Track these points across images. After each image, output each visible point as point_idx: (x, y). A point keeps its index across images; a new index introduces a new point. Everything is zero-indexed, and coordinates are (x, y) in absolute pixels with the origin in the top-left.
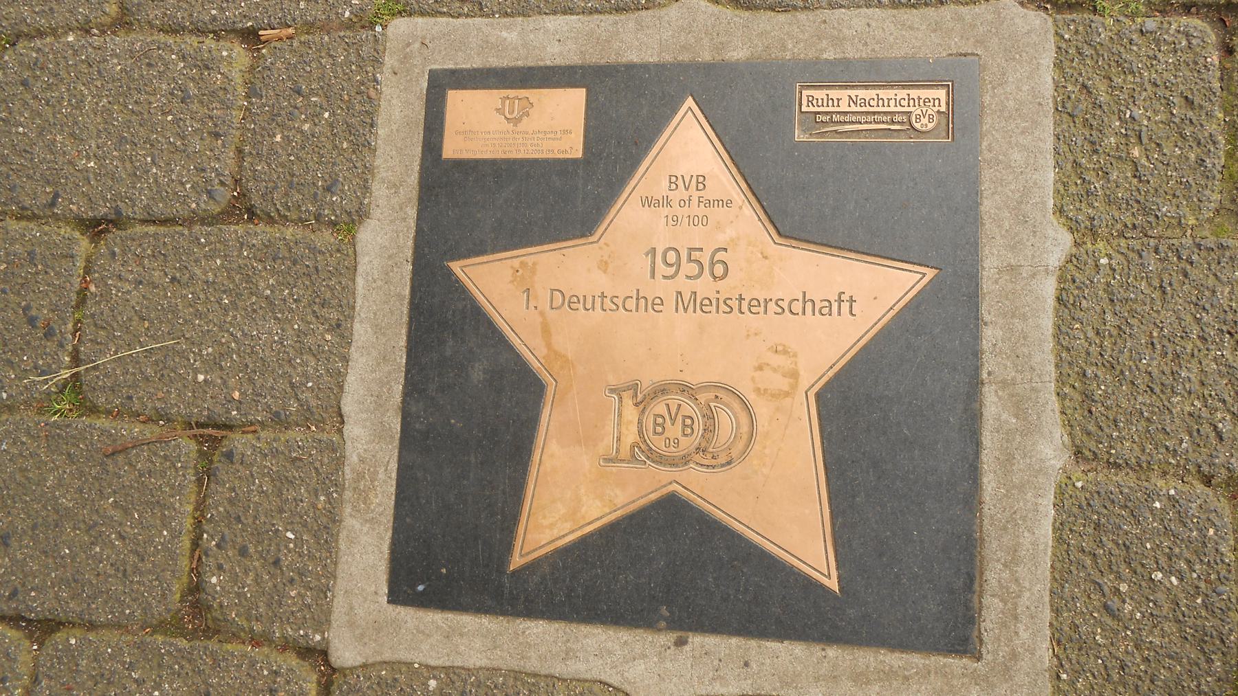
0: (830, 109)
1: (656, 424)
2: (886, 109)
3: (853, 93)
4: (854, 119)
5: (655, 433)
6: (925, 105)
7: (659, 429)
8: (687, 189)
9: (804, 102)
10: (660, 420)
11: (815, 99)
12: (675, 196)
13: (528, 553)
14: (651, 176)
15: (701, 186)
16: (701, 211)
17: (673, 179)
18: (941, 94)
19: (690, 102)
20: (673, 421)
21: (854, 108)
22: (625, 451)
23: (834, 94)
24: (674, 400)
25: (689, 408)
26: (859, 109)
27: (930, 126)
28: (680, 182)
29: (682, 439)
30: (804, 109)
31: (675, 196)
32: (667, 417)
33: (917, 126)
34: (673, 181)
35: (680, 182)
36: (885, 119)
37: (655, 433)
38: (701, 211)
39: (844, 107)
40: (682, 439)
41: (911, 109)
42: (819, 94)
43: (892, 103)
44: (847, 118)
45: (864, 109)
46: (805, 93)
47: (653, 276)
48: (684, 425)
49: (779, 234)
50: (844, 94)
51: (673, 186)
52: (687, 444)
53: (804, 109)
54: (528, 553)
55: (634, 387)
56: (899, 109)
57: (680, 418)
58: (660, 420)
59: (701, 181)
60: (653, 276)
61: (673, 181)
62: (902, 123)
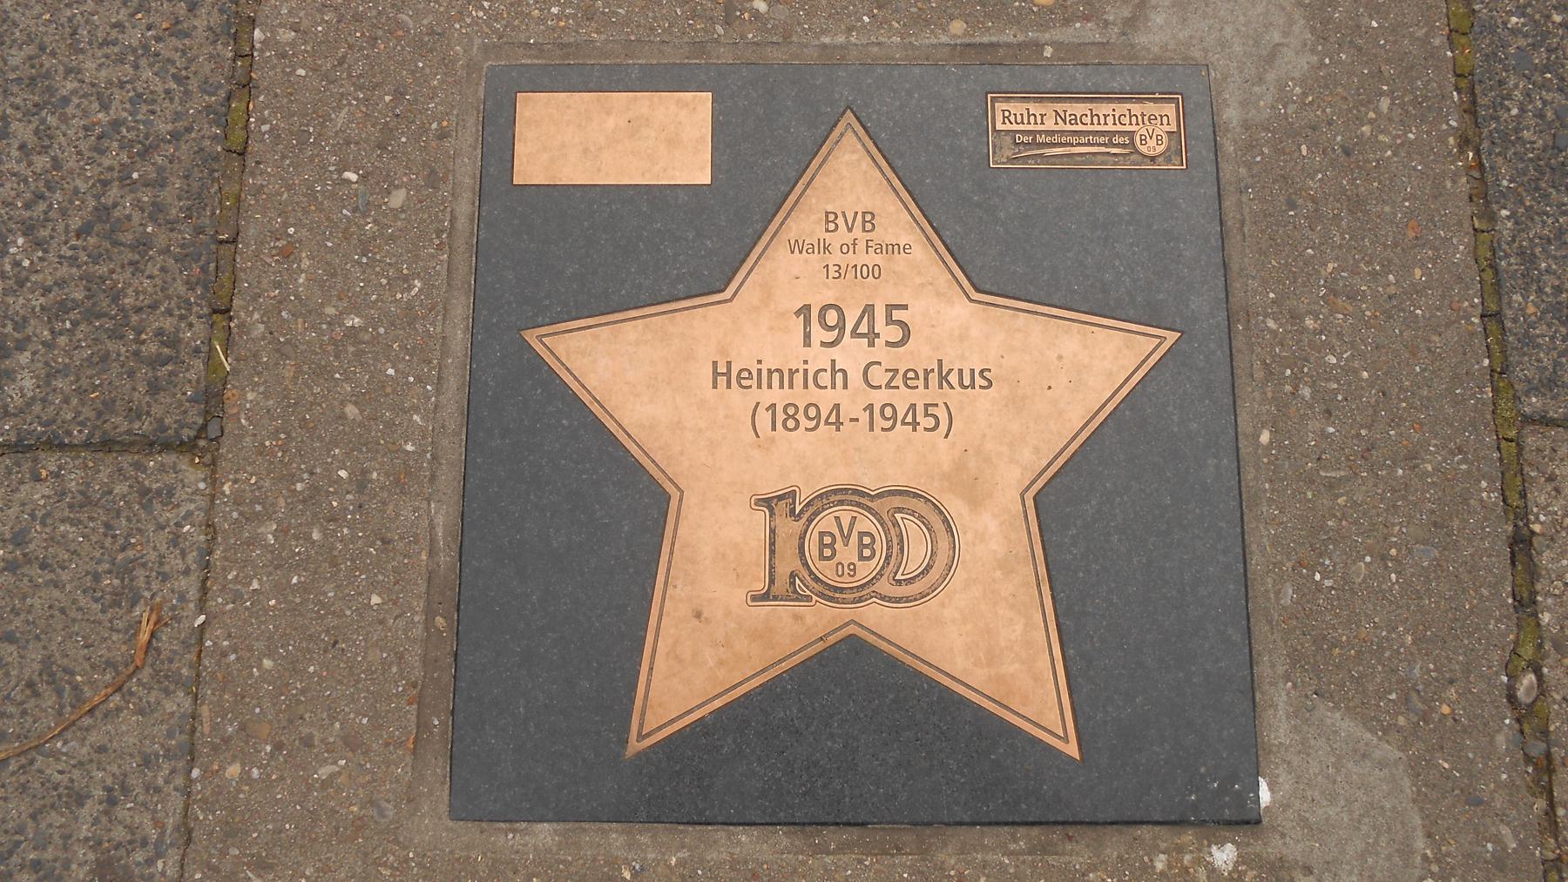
0: (1031, 127)
1: (822, 546)
3: (1059, 107)
4: (1063, 140)
5: (822, 557)
6: (1152, 127)
7: (827, 552)
8: (850, 230)
9: (999, 118)
10: (827, 540)
11: (1011, 115)
12: (835, 240)
15: (868, 226)
16: (873, 259)
17: (832, 217)
18: (1169, 110)
20: (846, 539)
21: (1061, 126)
22: (781, 585)
23: (1034, 108)
25: (866, 523)
26: (1069, 127)
27: (1160, 149)
28: (840, 221)
29: (859, 564)
30: (999, 126)
31: (835, 240)
33: (1143, 149)
34: (829, 218)
35: (840, 221)
36: (1102, 140)
37: (822, 557)
38: (873, 259)
39: (1049, 125)
40: (859, 564)
42: (1017, 108)
43: (1110, 120)
44: (1056, 139)
45: (1074, 128)
46: (999, 106)
47: (807, 341)
48: (862, 546)
49: (978, 290)
50: (1048, 109)
52: (865, 571)
53: (999, 126)
56: (1119, 128)
57: (854, 538)
59: (869, 220)
60: (807, 341)
61: (829, 218)
62: (1124, 146)
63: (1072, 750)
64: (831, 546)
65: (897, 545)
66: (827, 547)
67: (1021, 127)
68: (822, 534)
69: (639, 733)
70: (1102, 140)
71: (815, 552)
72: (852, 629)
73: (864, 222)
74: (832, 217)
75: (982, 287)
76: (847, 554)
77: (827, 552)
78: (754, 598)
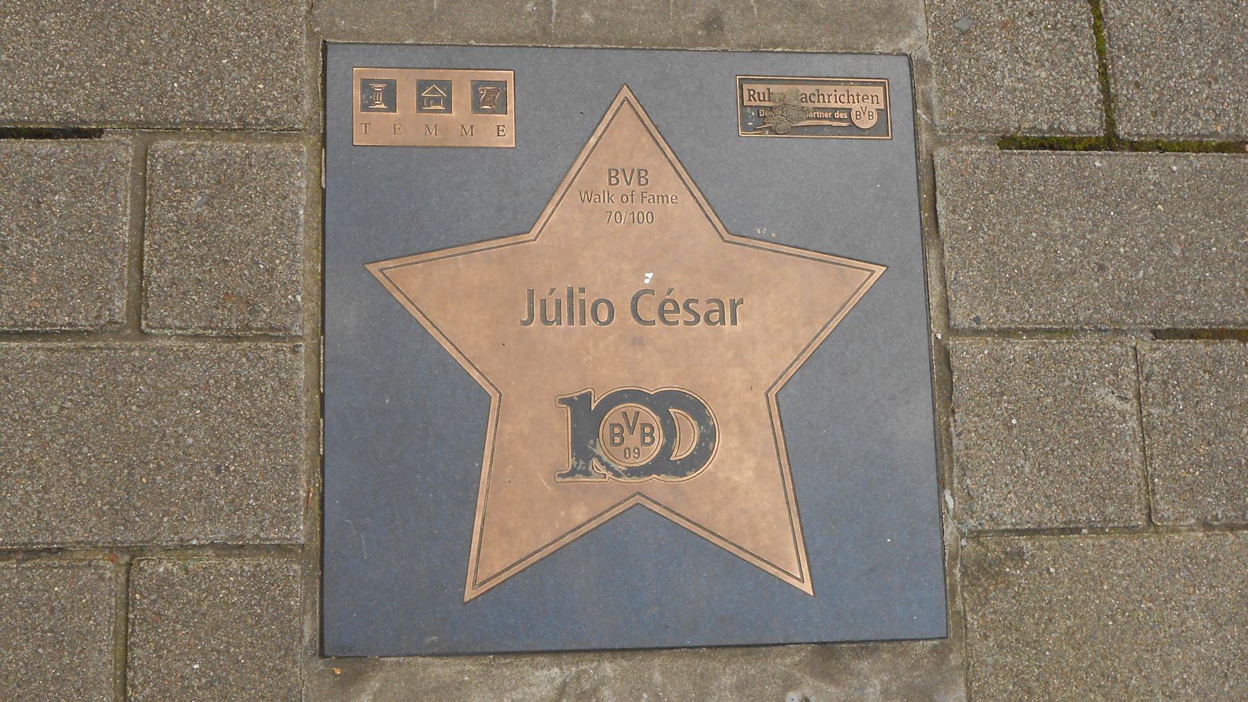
2: (829, 105)
10: (617, 430)
13: (485, 582)
14: (589, 169)
15: (643, 181)
17: (613, 173)
18: (879, 91)
19: (625, 92)
24: (631, 407)
25: (650, 416)
28: (620, 176)
32: (623, 422)
33: (857, 123)
34: (613, 174)
35: (620, 176)
36: (826, 115)
41: (848, 106)
42: (760, 88)
48: (644, 435)
51: (614, 181)
54: (485, 582)
55: (586, 398)
56: (839, 105)
57: (638, 427)
58: (617, 430)
61: (613, 174)
63: (807, 587)
64: (621, 435)
65: (670, 432)
66: (617, 437)
67: (763, 104)
68: (613, 426)
69: (474, 584)
70: (826, 115)
71: (608, 439)
72: (638, 499)
73: (639, 177)
74: (613, 173)
75: (732, 231)
76: (633, 440)
77: (617, 440)
78: (560, 475)
